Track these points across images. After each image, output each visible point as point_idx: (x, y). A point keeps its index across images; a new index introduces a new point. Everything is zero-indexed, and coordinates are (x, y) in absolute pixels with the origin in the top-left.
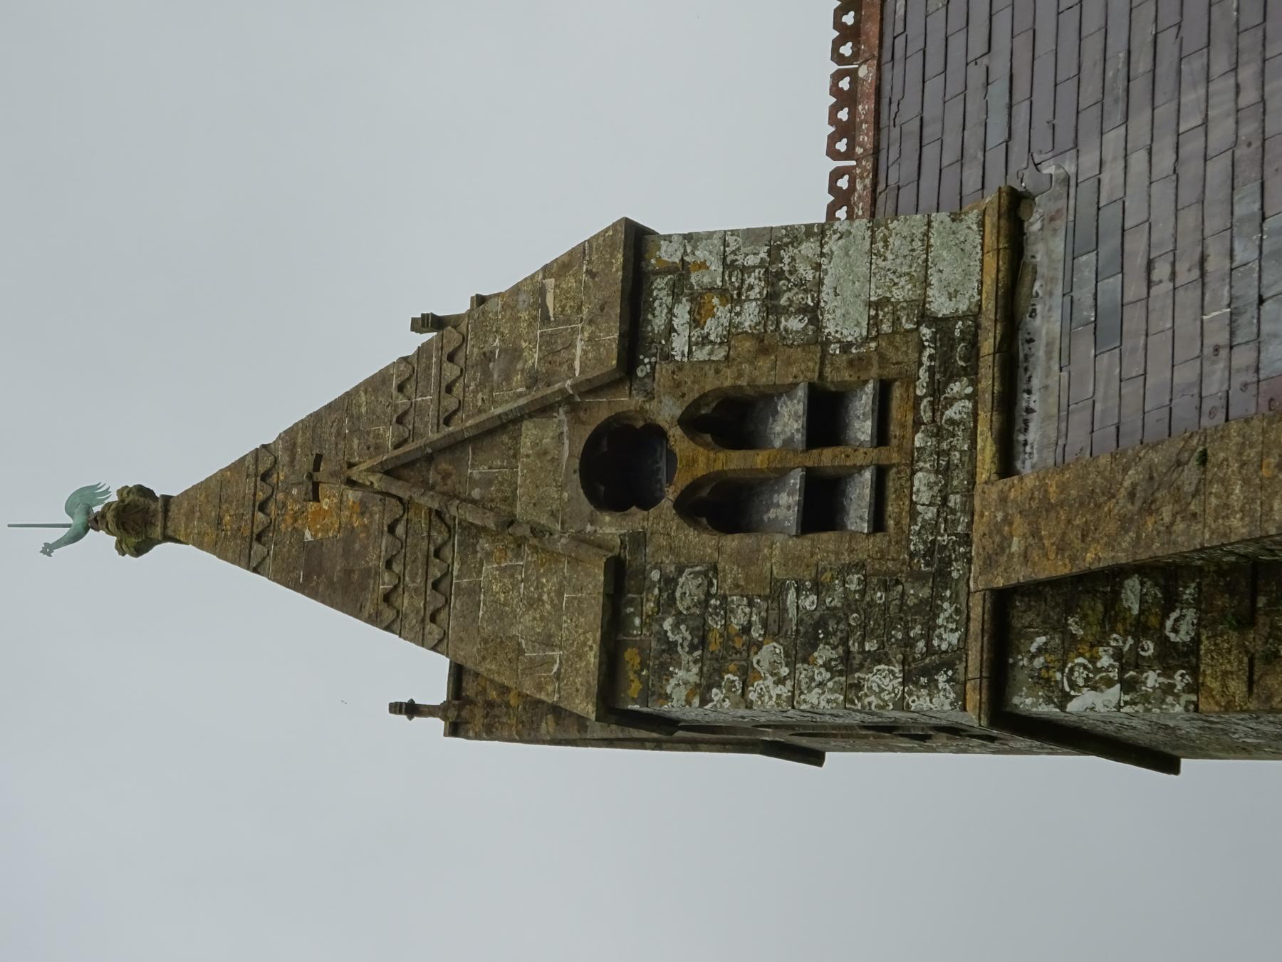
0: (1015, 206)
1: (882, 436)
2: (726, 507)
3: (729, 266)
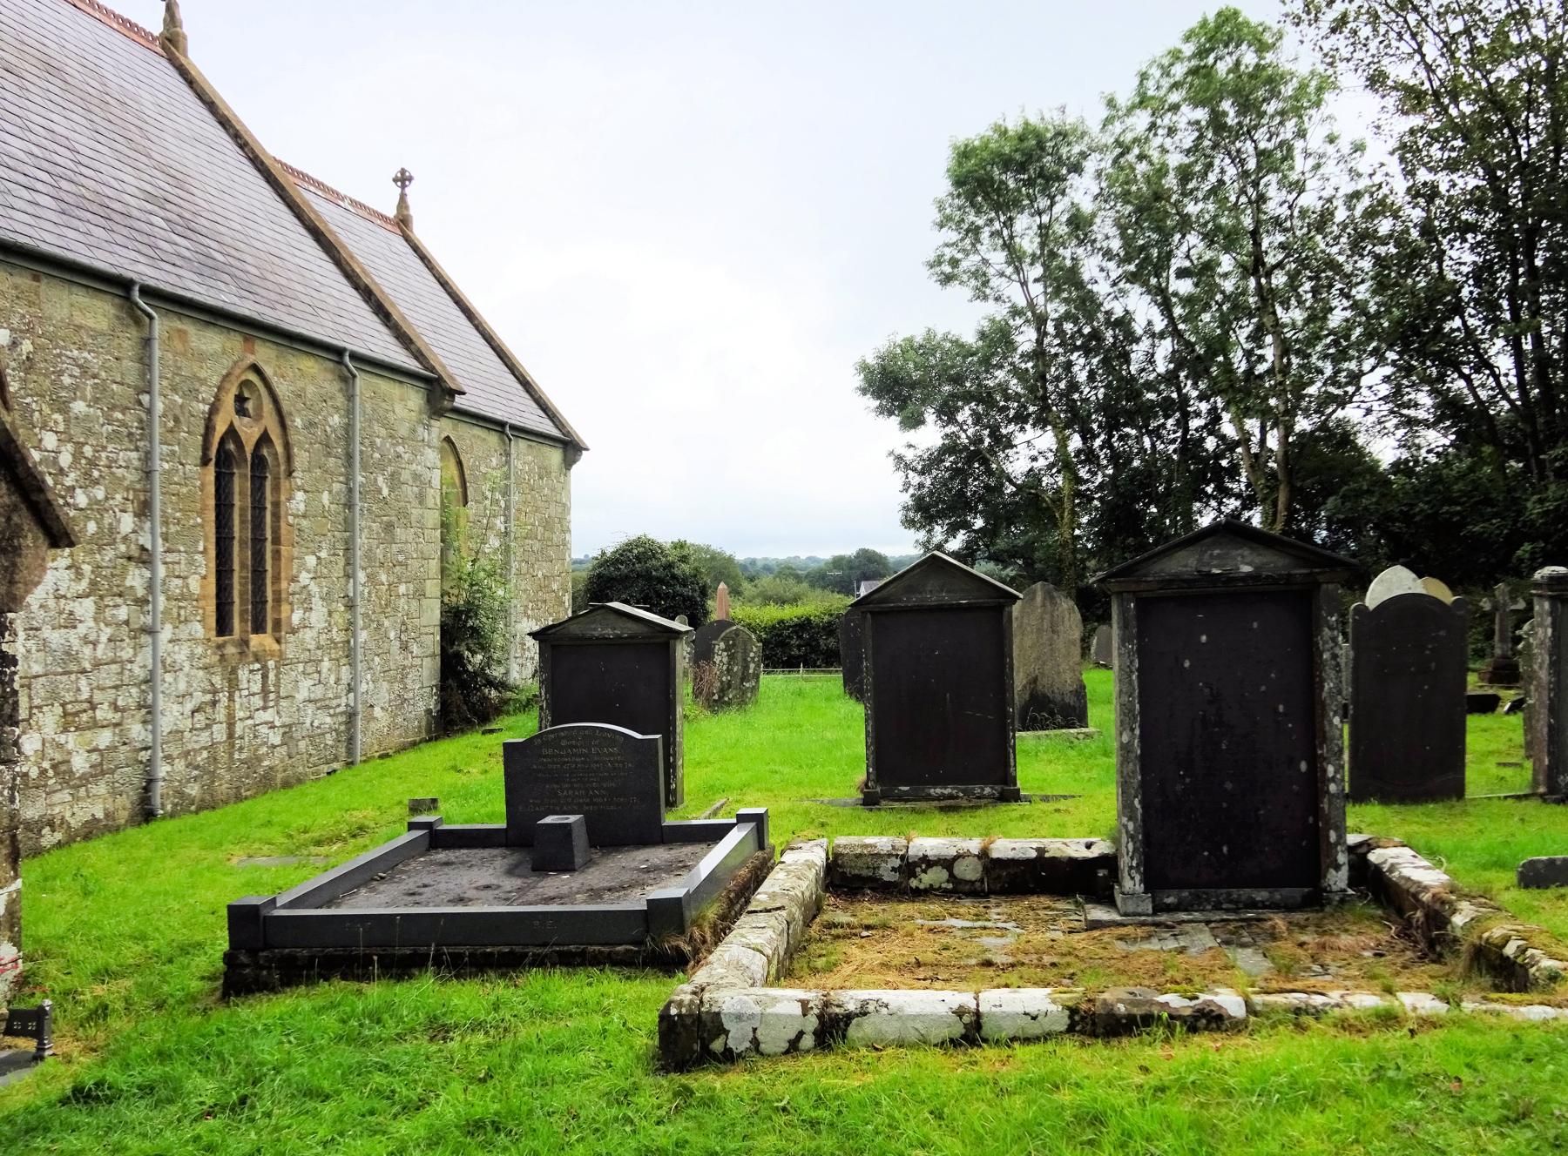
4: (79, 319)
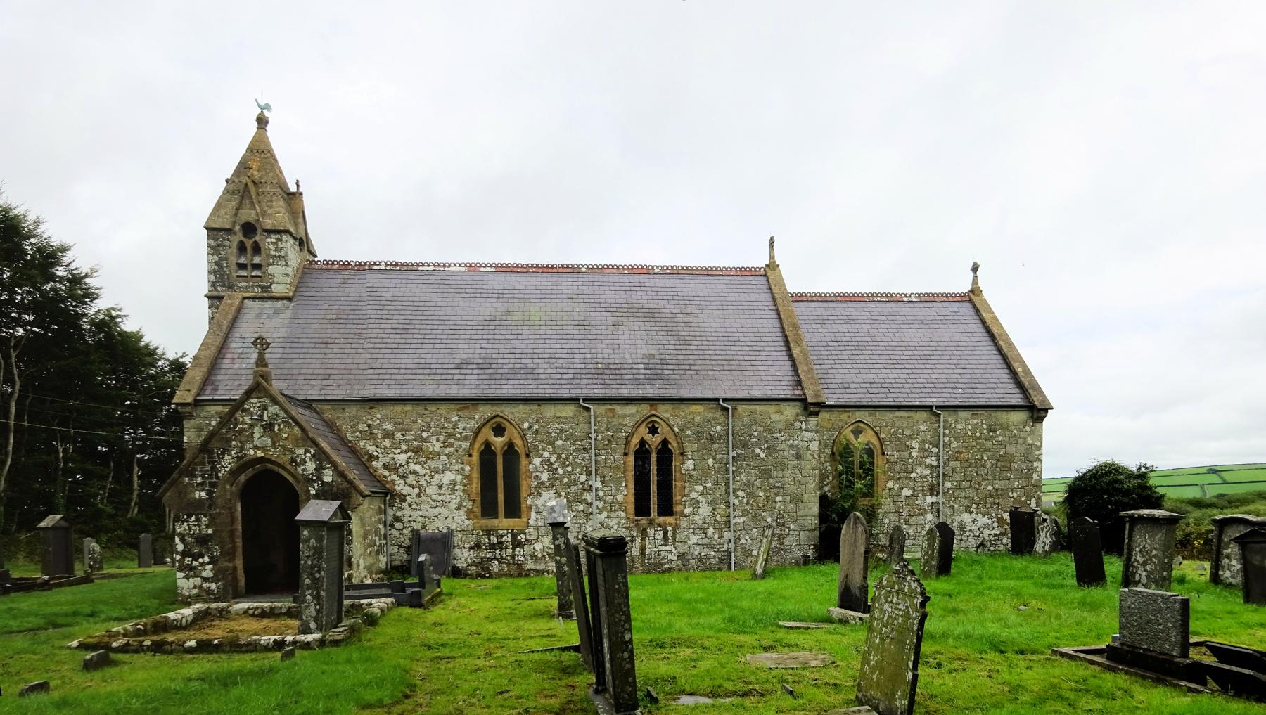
0: (290, 299)
2: (242, 249)
4: (558, 414)
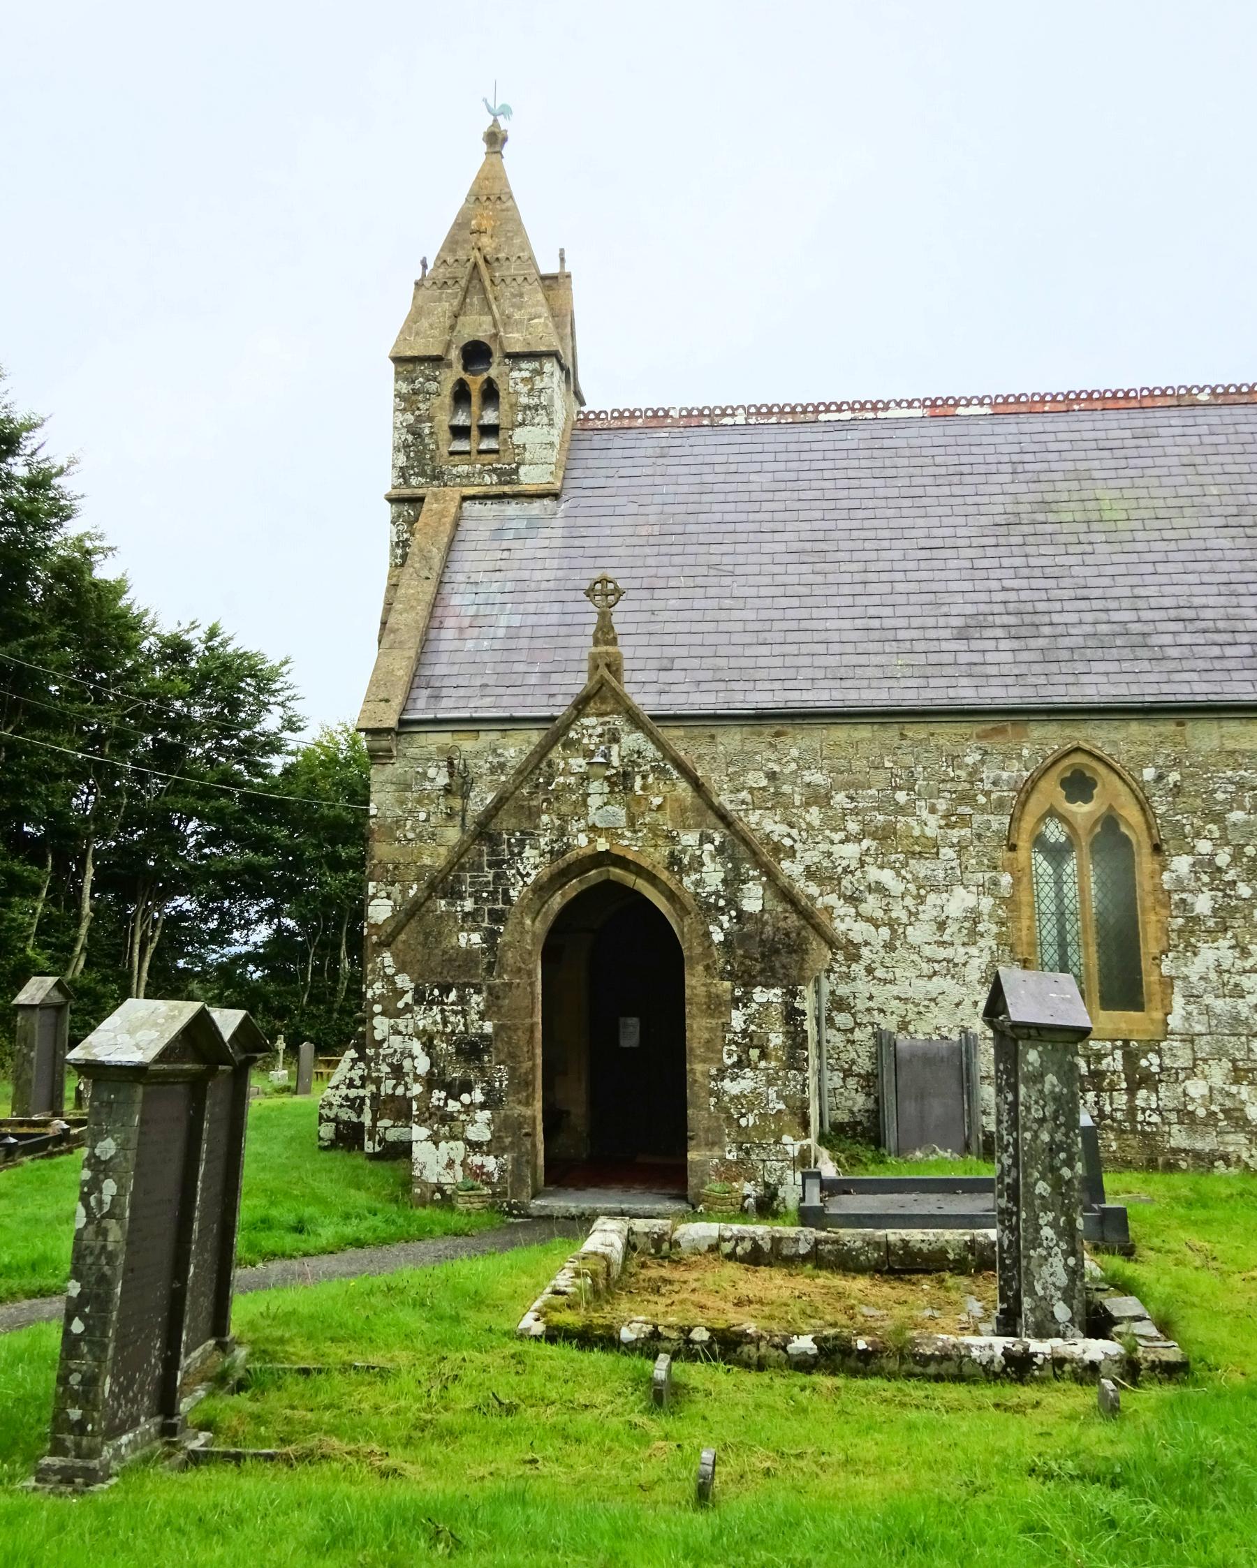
0: (556, 496)
1: (480, 452)
2: (461, 395)
3: (541, 391)
4: (1230, 745)
